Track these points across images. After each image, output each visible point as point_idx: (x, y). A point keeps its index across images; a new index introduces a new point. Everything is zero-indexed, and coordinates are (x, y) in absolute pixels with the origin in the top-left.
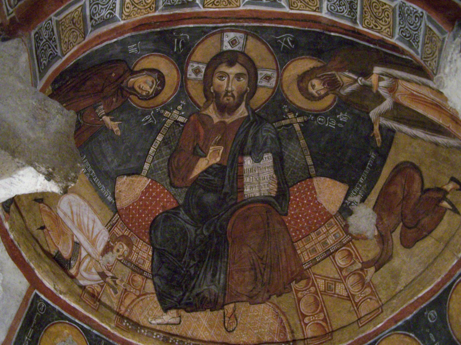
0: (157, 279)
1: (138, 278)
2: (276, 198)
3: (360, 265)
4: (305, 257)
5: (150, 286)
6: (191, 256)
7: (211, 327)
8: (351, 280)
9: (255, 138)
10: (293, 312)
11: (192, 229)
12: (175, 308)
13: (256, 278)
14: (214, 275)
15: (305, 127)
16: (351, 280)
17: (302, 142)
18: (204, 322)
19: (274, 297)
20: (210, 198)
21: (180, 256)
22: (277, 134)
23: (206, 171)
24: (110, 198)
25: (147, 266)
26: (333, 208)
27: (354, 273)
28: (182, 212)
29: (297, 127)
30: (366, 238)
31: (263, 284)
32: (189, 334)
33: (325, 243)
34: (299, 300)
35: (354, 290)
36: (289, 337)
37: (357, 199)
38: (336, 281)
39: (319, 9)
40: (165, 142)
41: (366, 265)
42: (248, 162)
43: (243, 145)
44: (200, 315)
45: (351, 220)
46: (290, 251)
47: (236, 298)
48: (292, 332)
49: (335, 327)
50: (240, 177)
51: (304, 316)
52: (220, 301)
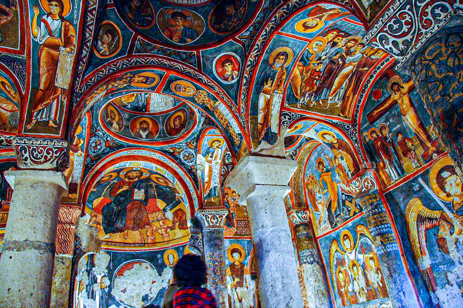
0: (104, 225)
1: (99, 226)
2: (144, 201)
3: (166, 227)
4: (151, 219)
5: (102, 227)
6: (115, 216)
7: (120, 237)
8: (163, 230)
9: (139, 185)
10: (145, 234)
11: (115, 208)
12: (109, 233)
13: (135, 223)
14: (121, 221)
15: (156, 186)
16: (163, 230)
17: (155, 189)
18: (118, 236)
19: (140, 229)
20: (122, 199)
21: (111, 216)
22: (147, 185)
23: (122, 192)
24: (91, 207)
25: (101, 221)
26: (161, 208)
27: (164, 228)
28: (113, 204)
29: (154, 185)
30: (169, 220)
31: (137, 225)
32: (114, 240)
33: (157, 217)
34: (147, 231)
35: (164, 233)
36: (143, 242)
37: (169, 209)
38: (159, 228)
39: (165, 174)
40: (109, 187)
41: (168, 227)
42: (136, 190)
43: (135, 186)
44: (116, 234)
45: (166, 213)
46: (146, 216)
47: (128, 228)
48: (144, 240)
49: (157, 241)
50: (133, 193)
51: (148, 236)
52: (123, 229)
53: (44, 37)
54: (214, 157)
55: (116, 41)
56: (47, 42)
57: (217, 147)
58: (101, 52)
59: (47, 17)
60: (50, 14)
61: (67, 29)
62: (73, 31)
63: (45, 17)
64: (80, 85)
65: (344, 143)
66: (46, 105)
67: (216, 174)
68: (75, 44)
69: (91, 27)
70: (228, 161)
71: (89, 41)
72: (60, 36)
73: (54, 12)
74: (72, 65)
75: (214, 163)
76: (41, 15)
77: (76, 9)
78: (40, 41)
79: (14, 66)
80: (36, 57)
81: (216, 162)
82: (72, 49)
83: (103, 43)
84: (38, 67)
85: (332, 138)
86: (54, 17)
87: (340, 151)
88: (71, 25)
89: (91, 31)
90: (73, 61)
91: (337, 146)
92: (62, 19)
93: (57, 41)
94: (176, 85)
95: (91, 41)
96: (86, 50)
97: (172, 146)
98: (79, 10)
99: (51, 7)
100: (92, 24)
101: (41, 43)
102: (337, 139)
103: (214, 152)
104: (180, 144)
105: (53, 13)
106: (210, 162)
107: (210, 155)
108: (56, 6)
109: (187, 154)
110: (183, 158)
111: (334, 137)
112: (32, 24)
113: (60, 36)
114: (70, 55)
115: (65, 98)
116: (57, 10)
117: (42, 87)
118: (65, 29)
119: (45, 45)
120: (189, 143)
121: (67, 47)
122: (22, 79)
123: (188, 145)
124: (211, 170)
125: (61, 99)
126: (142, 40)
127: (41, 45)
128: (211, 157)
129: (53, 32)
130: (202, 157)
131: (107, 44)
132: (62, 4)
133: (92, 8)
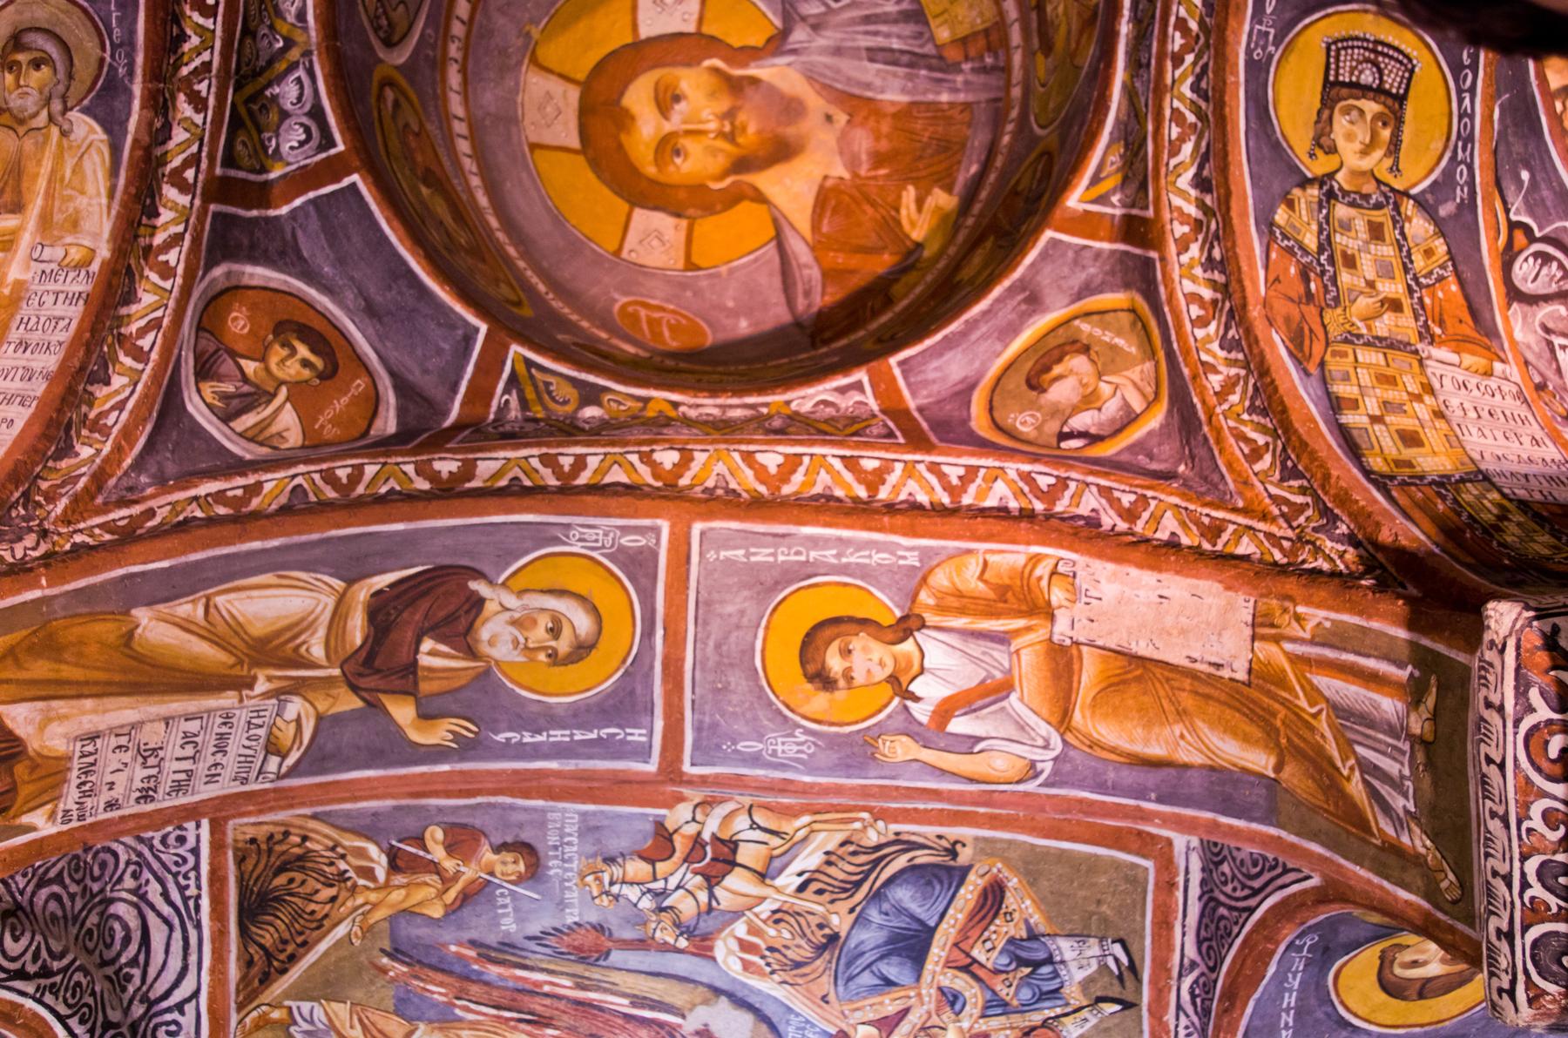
53: (1022, 726)
55: (1098, 332)
56: (1044, 712)
58: (1137, 405)
59: (917, 699)
60: (899, 685)
61: (952, 602)
62: (959, 571)
63: (921, 712)
64: (1264, 517)
66: (1347, 746)
68: (1021, 560)
69: (954, 473)
71: (1027, 478)
72: (1002, 639)
73: (881, 664)
74: (1134, 572)
76: (916, 728)
77: (838, 556)
78: (1046, 747)
79: (1231, 908)
80: (1129, 777)
82: (1054, 573)
83: (1089, 400)
84: (1172, 771)
86: (910, 664)
88: (932, 580)
89: (972, 471)
90: (1110, 566)
92: (908, 626)
93: (1028, 660)
95: (1026, 467)
96: (1077, 498)
98: (840, 539)
99: (859, 677)
100: (934, 468)
101: (1056, 741)
105: (888, 671)
108: (846, 652)
112: (972, 780)
113: (1002, 639)
114: (1082, 581)
115: (1298, 618)
116: (865, 650)
117: (1260, 761)
118: (962, 611)
119: (1063, 721)
121: (1049, 603)
122: (1267, 876)
125: (1302, 641)
126: (1096, 180)
127: (1064, 742)
129: (992, 677)
131: (1100, 376)
132: (836, 621)
133: (848, 476)
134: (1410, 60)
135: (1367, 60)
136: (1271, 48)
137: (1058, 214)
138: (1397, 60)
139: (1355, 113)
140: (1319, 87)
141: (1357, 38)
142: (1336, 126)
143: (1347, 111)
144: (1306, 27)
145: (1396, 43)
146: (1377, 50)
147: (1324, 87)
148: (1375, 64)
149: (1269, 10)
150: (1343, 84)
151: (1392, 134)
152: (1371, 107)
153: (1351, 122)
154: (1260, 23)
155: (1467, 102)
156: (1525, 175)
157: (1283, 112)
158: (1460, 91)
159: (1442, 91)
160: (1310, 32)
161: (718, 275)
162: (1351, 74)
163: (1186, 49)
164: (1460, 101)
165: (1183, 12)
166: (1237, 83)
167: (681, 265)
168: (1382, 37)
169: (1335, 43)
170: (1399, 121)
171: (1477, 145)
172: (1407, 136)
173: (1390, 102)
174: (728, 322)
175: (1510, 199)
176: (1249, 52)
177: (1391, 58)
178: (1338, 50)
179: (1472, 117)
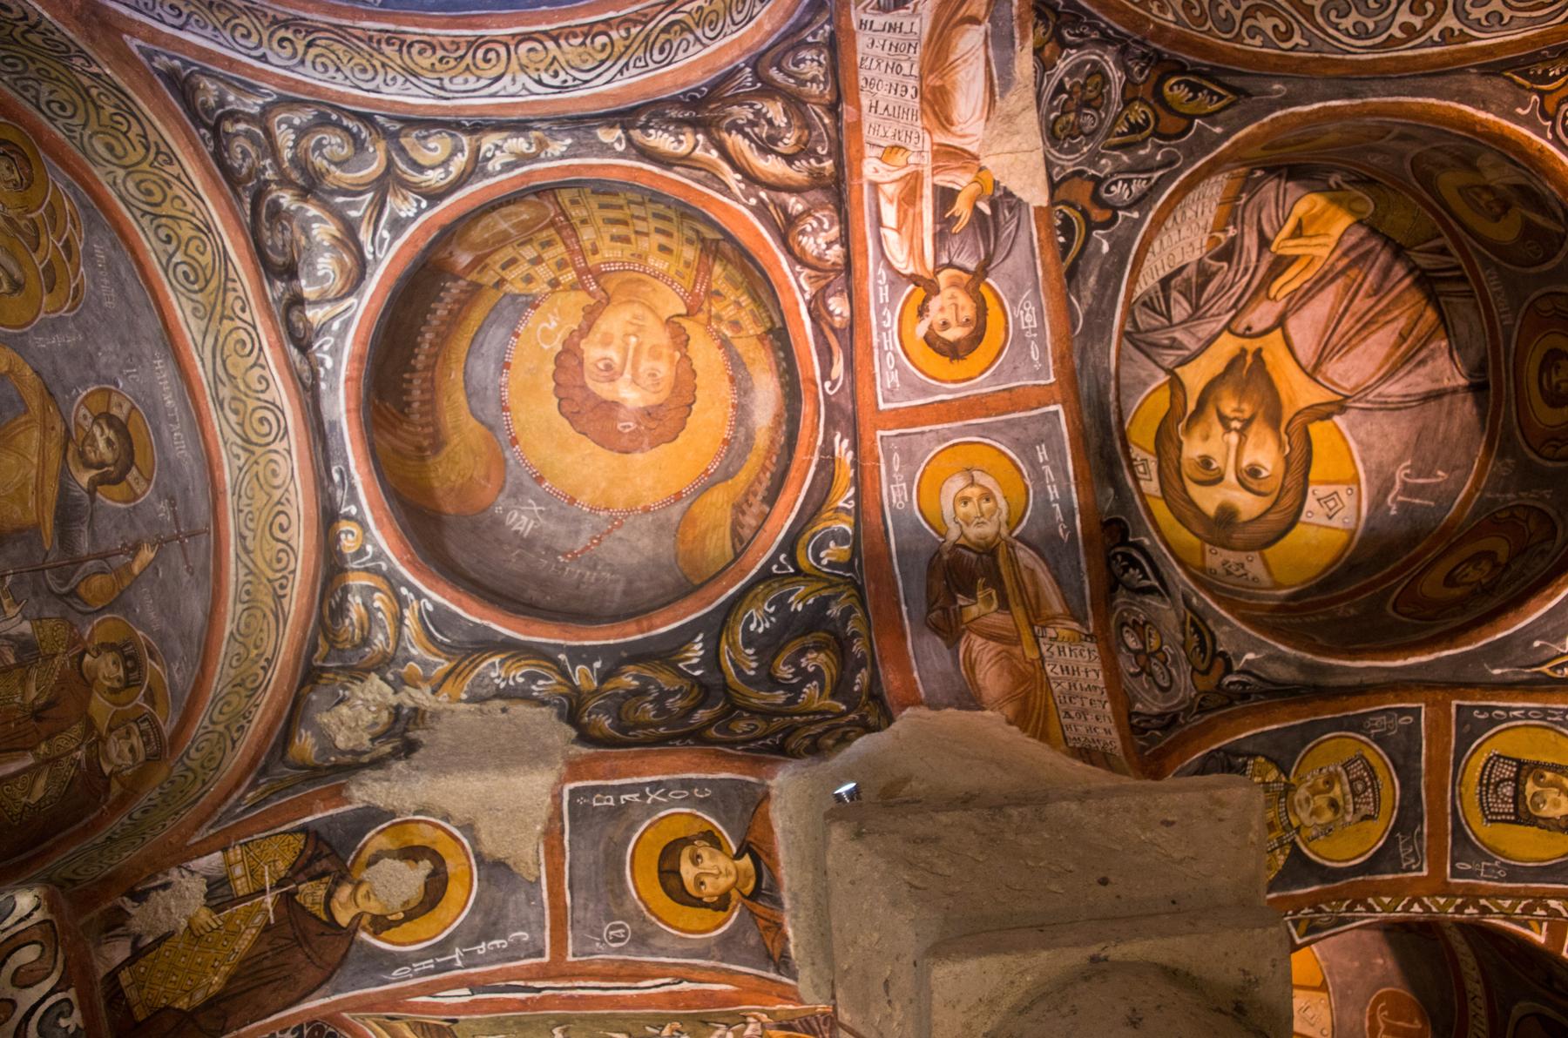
54: (928, 192)
57: (932, 289)
65: (312, 974)
67: (891, 78)
70: (757, 113)
75: (919, 156)
81: (900, 159)
85: (374, 907)
87: (269, 900)
91: (311, 893)
94: (1377, 802)
97: (1191, 156)
102: (350, 932)
103: (940, 238)
104: (1139, 186)
106: (949, 155)
107: (962, 209)
109: (1088, 121)
110: (1106, 80)
111: (380, 924)
120: (1098, 215)
123: (1096, 199)
124: (937, 104)
128: (946, 197)
130: (1014, 186)
134: (1491, 758)
135: (1495, 791)
136: (1496, 864)
137: (1551, 949)
138: (1492, 768)
139: (1536, 799)
140: (1522, 828)
141: (1481, 799)
142: (1550, 814)
143: (1537, 806)
144: (1477, 838)
145: (1479, 769)
146: (1488, 784)
147: (1520, 824)
148: (1497, 785)
149: (1469, 867)
150: (1516, 808)
151: (1549, 770)
152: (1530, 788)
153: (1544, 802)
154: (1479, 872)
155: (1516, 713)
156: (1537, 644)
157: (1546, 856)
158: (1509, 719)
159: (1511, 733)
160: (1481, 835)
161: (1329, 968)
162: (1507, 803)
163: (1476, 905)
164: (1516, 718)
165: (1451, 910)
166: (1526, 888)
167: (1325, 995)
168: (1477, 780)
169: (1486, 816)
170: (1537, 765)
171: (1549, 706)
172: (1549, 760)
173: (1524, 773)
174: (1378, 972)
175: (1555, 653)
176: (1501, 880)
177: (1490, 773)
178: (1492, 813)
179: (1528, 710)
